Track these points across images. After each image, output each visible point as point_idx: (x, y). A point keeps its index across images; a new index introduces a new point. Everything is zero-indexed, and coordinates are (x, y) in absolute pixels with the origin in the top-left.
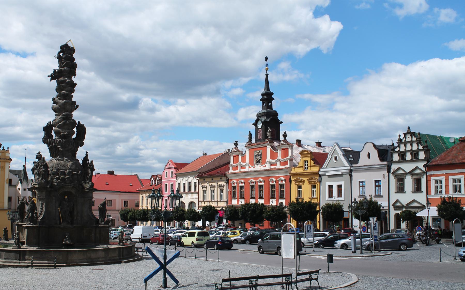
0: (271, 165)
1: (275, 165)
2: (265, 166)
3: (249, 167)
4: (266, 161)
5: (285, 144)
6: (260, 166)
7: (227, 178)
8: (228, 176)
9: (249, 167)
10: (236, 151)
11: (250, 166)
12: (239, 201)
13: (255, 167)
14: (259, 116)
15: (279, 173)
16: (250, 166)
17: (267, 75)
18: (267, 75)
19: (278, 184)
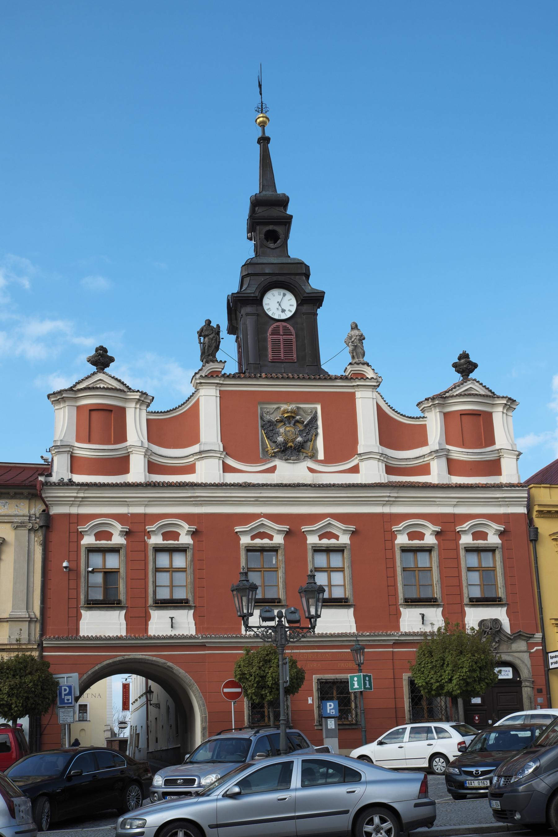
0: (390, 470)
1: (425, 470)
2: (355, 470)
3: (227, 468)
4: (360, 450)
5: (484, 396)
6: (311, 470)
7: (47, 506)
8: (49, 494)
9: (227, 468)
10: (116, 390)
11: (231, 462)
12: (147, 618)
13: (272, 470)
14: (267, 271)
15: (461, 502)
16: (231, 462)
17: (264, 141)
18: (264, 141)
19: (457, 545)
